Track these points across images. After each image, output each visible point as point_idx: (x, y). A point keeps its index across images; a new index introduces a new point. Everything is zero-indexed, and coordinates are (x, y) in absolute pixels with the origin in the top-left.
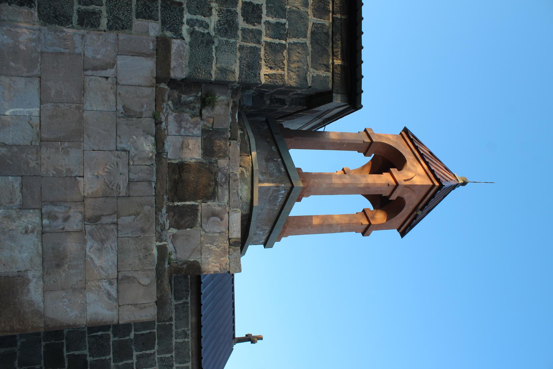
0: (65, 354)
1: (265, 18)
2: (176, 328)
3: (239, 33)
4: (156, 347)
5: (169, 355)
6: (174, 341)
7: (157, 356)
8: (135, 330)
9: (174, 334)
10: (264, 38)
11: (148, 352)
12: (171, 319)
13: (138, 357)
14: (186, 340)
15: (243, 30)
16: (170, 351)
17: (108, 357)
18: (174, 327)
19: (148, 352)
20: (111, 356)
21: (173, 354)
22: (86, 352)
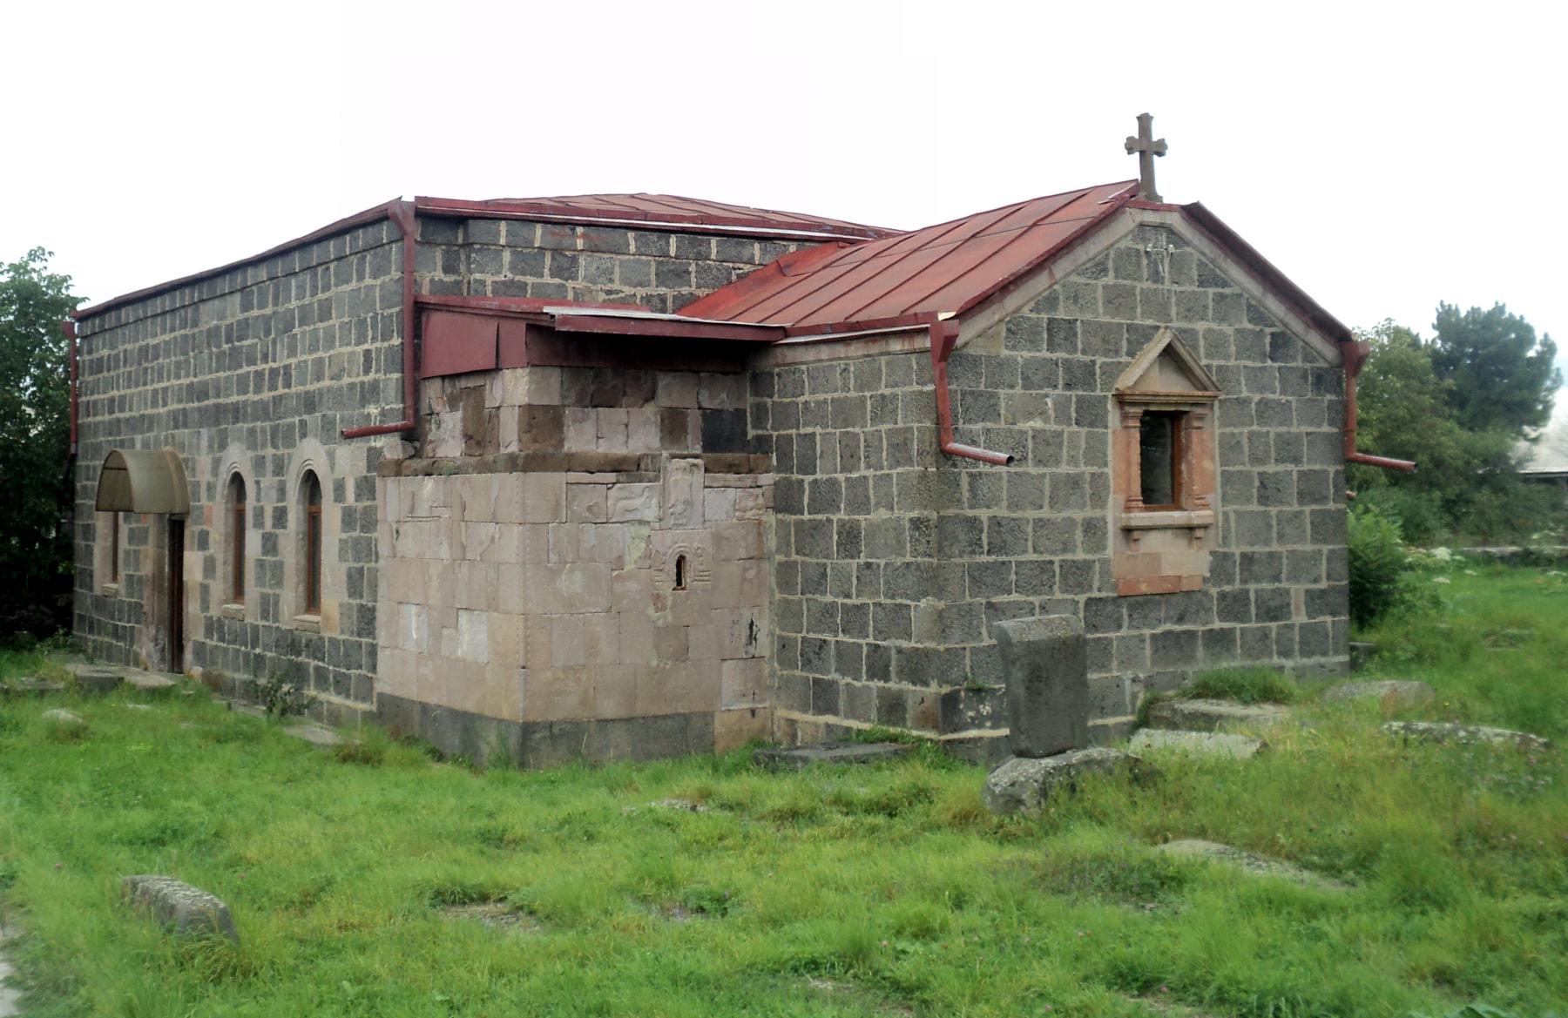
0: (854, 601)
1: (367, 346)
2: (836, 391)
3: (377, 376)
4: (857, 430)
5: (869, 402)
6: (853, 394)
7: (869, 429)
8: (836, 472)
9: (844, 394)
10: (378, 344)
11: (862, 446)
12: (825, 401)
13: (868, 467)
14: (852, 369)
15: (377, 371)
16: (863, 400)
17: (863, 524)
18: (836, 395)
19: (862, 446)
20: (861, 517)
21: (868, 394)
22: (854, 563)
